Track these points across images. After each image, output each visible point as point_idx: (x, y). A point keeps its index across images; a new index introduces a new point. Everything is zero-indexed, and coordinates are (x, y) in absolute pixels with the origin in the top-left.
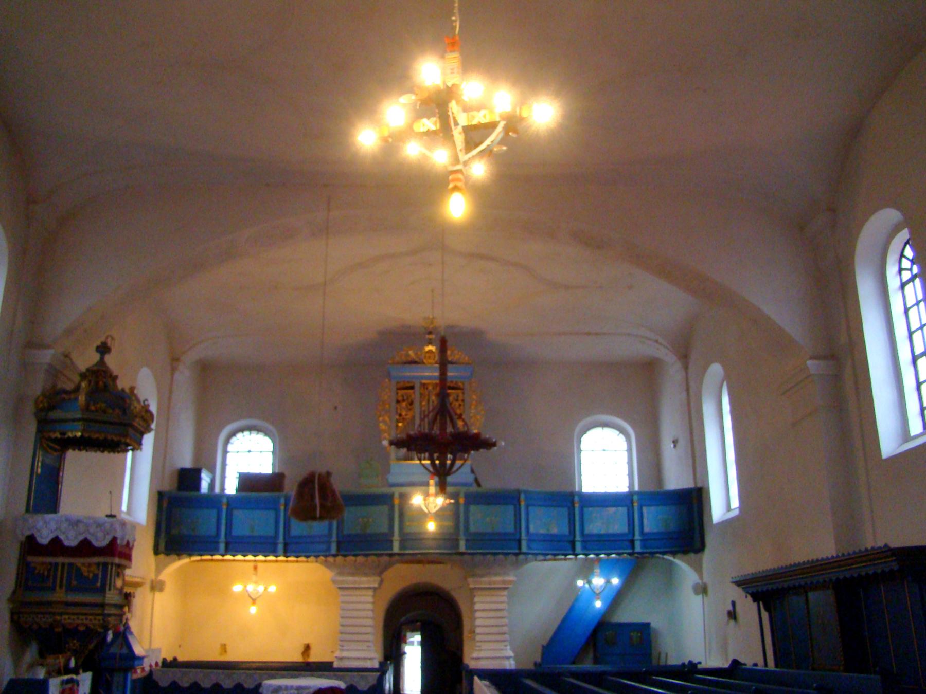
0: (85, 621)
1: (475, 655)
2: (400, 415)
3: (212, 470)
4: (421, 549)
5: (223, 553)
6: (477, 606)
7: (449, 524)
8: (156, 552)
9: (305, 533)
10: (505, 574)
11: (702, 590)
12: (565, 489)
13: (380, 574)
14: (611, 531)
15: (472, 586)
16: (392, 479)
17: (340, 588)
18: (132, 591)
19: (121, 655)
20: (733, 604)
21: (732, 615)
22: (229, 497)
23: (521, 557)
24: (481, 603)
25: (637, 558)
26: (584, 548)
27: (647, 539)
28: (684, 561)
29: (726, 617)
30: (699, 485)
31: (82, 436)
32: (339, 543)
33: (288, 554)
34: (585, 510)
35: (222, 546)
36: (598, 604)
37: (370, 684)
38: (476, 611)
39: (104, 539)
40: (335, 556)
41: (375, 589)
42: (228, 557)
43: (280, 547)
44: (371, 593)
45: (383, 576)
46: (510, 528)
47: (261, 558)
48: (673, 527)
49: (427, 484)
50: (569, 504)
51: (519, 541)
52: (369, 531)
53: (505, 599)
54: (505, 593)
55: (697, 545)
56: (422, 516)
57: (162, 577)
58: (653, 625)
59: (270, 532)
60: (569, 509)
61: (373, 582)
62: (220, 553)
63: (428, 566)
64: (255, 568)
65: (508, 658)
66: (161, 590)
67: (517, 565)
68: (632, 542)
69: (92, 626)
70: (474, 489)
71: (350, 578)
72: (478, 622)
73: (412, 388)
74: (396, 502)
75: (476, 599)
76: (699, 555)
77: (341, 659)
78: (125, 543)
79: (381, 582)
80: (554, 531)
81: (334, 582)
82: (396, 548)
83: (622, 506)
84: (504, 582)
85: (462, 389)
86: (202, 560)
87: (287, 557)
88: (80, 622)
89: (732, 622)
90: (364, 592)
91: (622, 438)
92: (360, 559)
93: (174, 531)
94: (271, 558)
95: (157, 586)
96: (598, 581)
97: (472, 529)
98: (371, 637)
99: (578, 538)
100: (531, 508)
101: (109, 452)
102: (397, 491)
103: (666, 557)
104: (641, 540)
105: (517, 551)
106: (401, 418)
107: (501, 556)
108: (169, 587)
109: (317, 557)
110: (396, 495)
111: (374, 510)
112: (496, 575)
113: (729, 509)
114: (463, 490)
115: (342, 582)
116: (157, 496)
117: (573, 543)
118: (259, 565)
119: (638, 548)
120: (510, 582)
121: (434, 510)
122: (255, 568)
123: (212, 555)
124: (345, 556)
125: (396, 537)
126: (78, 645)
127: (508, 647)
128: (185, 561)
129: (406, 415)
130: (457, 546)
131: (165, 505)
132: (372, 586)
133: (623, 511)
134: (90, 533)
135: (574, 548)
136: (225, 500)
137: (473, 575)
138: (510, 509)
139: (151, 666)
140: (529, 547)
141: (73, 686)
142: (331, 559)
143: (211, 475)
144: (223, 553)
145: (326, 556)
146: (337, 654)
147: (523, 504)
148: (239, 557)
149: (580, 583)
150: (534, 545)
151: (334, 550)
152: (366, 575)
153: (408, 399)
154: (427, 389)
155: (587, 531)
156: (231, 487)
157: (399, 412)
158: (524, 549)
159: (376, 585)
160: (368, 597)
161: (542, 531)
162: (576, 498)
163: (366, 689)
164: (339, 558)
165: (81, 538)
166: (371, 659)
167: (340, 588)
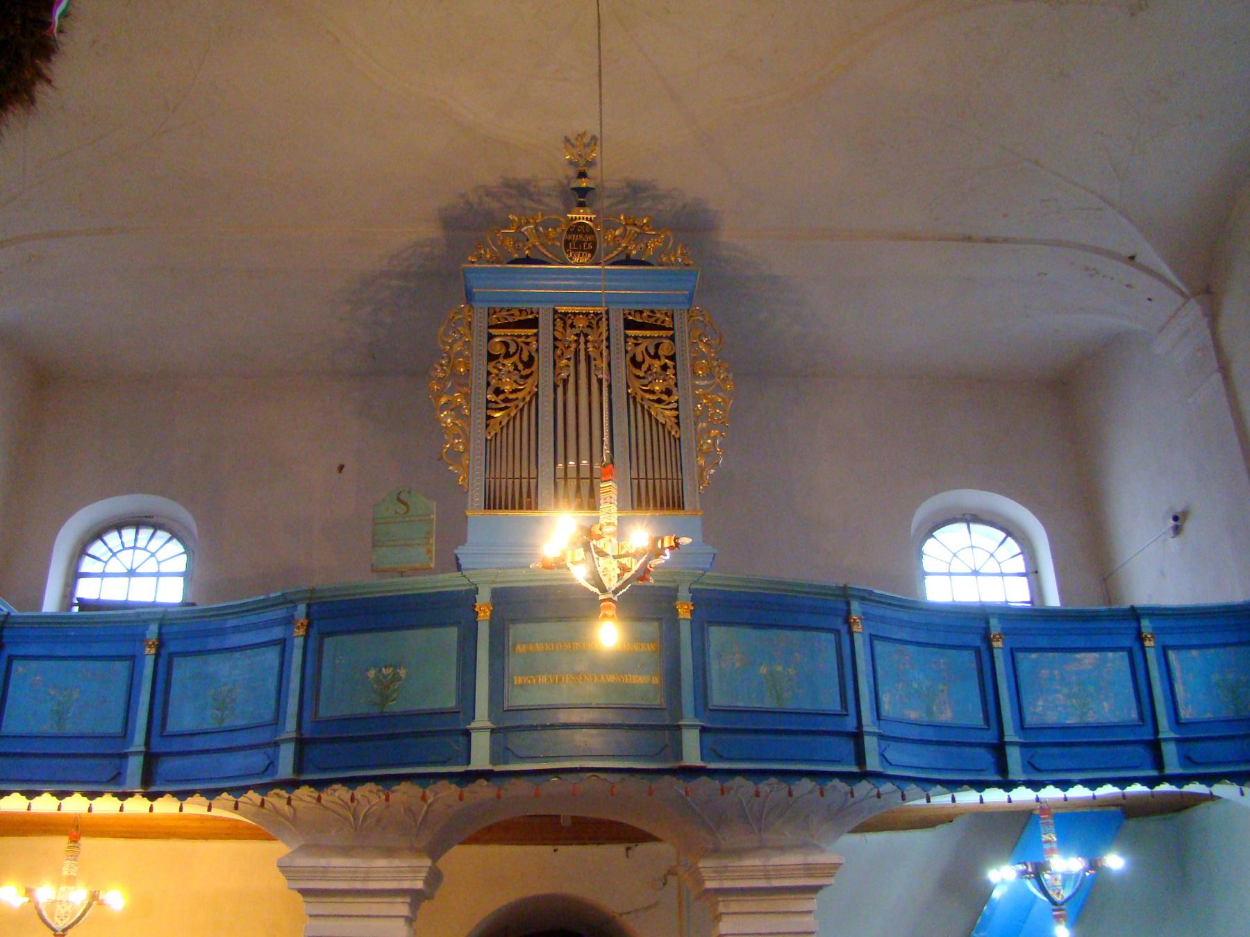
2: (498, 392)
13: (435, 852)
14: (1091, 718)
15: (709, 885)
17: (304, 892)
23: (864, 787)
26: (1030, 765)
32: (302, 744)
33: (153, 789)
34: (1020, 656)
40: (291, 785)
41: (416, 898)
43: (135, 765)
51: (857, 736)
52: (394, 707)
68: (1155, 746)
71: (338, 862)
73: (533, 323)
79: (434, 878)
81: (284, 869)
82: (481, 758)
84: (809, 869)
85: (672, 329)
91: (1012, 546)
94: (107, 805)
97: (718, 698)
105: (855, 769)
106: (502, 397)
107: (807, 784)
111: (417, 639)
112: (782, 849)
115: (314, 873)
117: (999, 749)
124: (319, 785)
129: (514, 391)
130: (679, 755)
132: (406, 885)
135: (1002, 767)
137: (716, 852)
142: (276, 799)
145: (263, 789)
152: (389, 852)
153: (519, 350)
154: (572, 326)
155: (1030, 720)
157: (493, 382)
158: (873, 763)
159: (419, 885)
161: (913, 715)
162: (995, 626)
164: (304, 792)
167: (304, 892)
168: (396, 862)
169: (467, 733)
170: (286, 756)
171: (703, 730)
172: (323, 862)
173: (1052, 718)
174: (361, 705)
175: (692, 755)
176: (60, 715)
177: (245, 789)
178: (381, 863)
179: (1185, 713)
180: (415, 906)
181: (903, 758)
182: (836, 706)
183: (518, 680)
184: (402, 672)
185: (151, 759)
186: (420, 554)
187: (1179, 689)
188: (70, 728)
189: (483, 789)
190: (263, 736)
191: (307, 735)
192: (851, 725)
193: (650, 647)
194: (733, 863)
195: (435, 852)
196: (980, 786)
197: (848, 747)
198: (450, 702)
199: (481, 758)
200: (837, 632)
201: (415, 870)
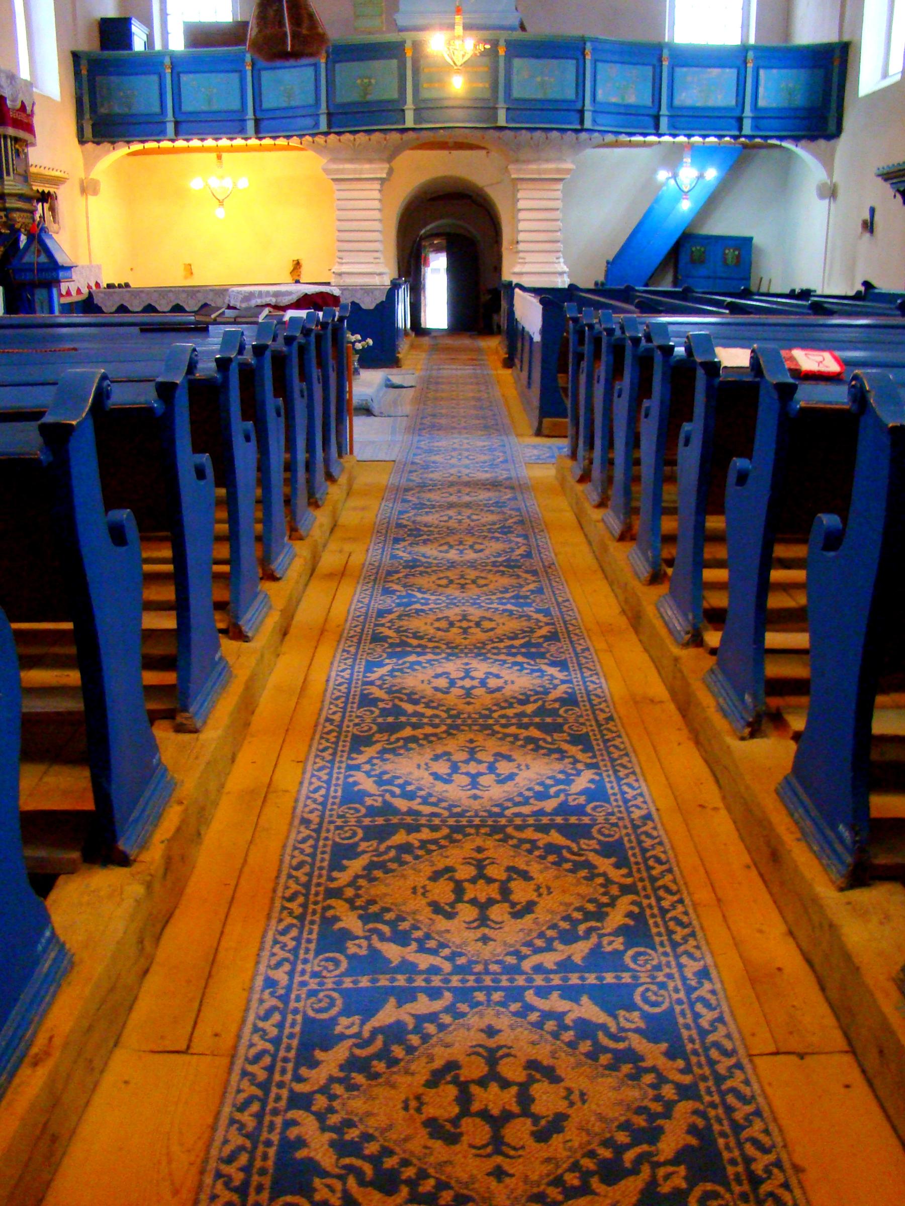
1: (517, 269)
3: (148, 23)
4: (444, 122)
5: (174, 137)
6: (521, 205)
7: (483, 85)
8: (82, 141)
9: (284, 105)
10: (560, 160)
11: (830, 193)
12: (653, 39)
13: (390, 159)
14: (711, 103)
15: (513, 176)
16: (401, 21)
18: (52, 191)
20: (872, 211)
21: (869, 226)
22: (173, 56)
23: (584, 135)
24: (526, 199)
25: (745, 146)
27: (760, 116)
28: (808, 151)
29: (860, 229)
30: (846, 38)
32: (330, 115)
35: (170, 127)
36: (686, 207)
37: (378, 301)
38: (519, 221)
40: (326, 134)
42: (180, 143)
43: (250, 125)
44: (377, 186)
45: (393, 164)
46: (570, 94)
47: (224, 142)
48: (799, 101)
49: (451, 27)
50: (655, 62)
51: (581, 112)
52: (369, 98)
53: (558, 194)
54: (560, 186)
55: (832, 128)
56: (446, 69)
57: (94, 175)
58: (758, 240)
59: (236, 105)
60: (654, 66)
61: (379, 170)
62: (169, 137)
63: (455, 153)
64: (219, 158)
65: (561, 274)
66: (95, 192)
67: (578, 146)
68: (740, 120)
70: (518, 35)
71: (348, 166)
72: (522, 226)
74: (409, 54)
75: (519, 195)
76: (833, 142)
77: (340, 274)
79: (391, 172)
80: (632, 100)
81: (325, 170)
82: (409, 123)
83: (730, 67)
84: (558, 171)
86: (144, 152)
87: (260, 139)
89: (867, 235)
90: (367, 185)
92: (361, 138)
93: (103, 110)
94: (239, 142)
95: (88, 188)
96: (688, 173)
97: (516, 94)
98: (377, 246)
99: (664, 111)
100: (600, 65)
102: (409, 37)
103: (785, 144)
104: (753, 118)
105: (579, 127)
107: (555, 134)
108: (105, 188)
109: (301, 136)
110: (408, 46)
111: (377, 65)
112: (547, 161)
113: (885, 75)
114: (503, 36)
115: (337, 171)
116: (70, 60)
117: (657, 118)
118: (225, 156)
119: (747, 130)
120: (568, 171)
121: (460, 62)
122: (219, 158)
123: (158, 141)
124: (339, 134)
125: (409, 105)
127: (562, 260)
128: (122, 151)
131: (84, 72)
132: (379, 176)
133: (730, 75)
135: (657, 126)
136: (167, 61)
137: (517, 161)
138: (571, 65)
139: (89, 287)
140: (594, 122)
142: (320, 140)
143: (146, 30)
144: (174, 137)
145: (313, 135)
146: (336, 268)
147: (588, 57)
148: (195, 143)
149: (662, 175)
150: (601, 119)
151: (323, 127)
152: (370, 161)
155: (676, 103)
156: (177, 44)
158: (588, 124)
159: (384, 176)
160: (373, 192)
161: (614, 100)
162: (666, 53)
163: (372, 307)
164: (332, 137)
166: (380, 274)
167: (334, 180)
168: (373, 166)
169: (403, 111)
170: (323, 120)
171: (508, 109)
172: (341, 166)
173: (689, 103)
174: (353, 96)
175: (502, 121)
176: (210, 101)
177: (304, 135)
178: (367, 166)
179: (761, 103)
180: (382, 185)
181: (605, 122)
182: (573, 97)
183: (425, 85)
184: (373, 81)
185: (257, 121)
186: (376, 23)
187: (761, 90)
188: (215, 108)
189: (411, 134)
190: (311, 111)
191: (332, 111)
192: (579, 106)
193: (486, 69)
194: (524, 167)
195: (390, 159)
196: (645, 135)
197: (575, 117)
198: (395, 96)
199: (409, 123)
200: (577, 59)
201: (382, 169)
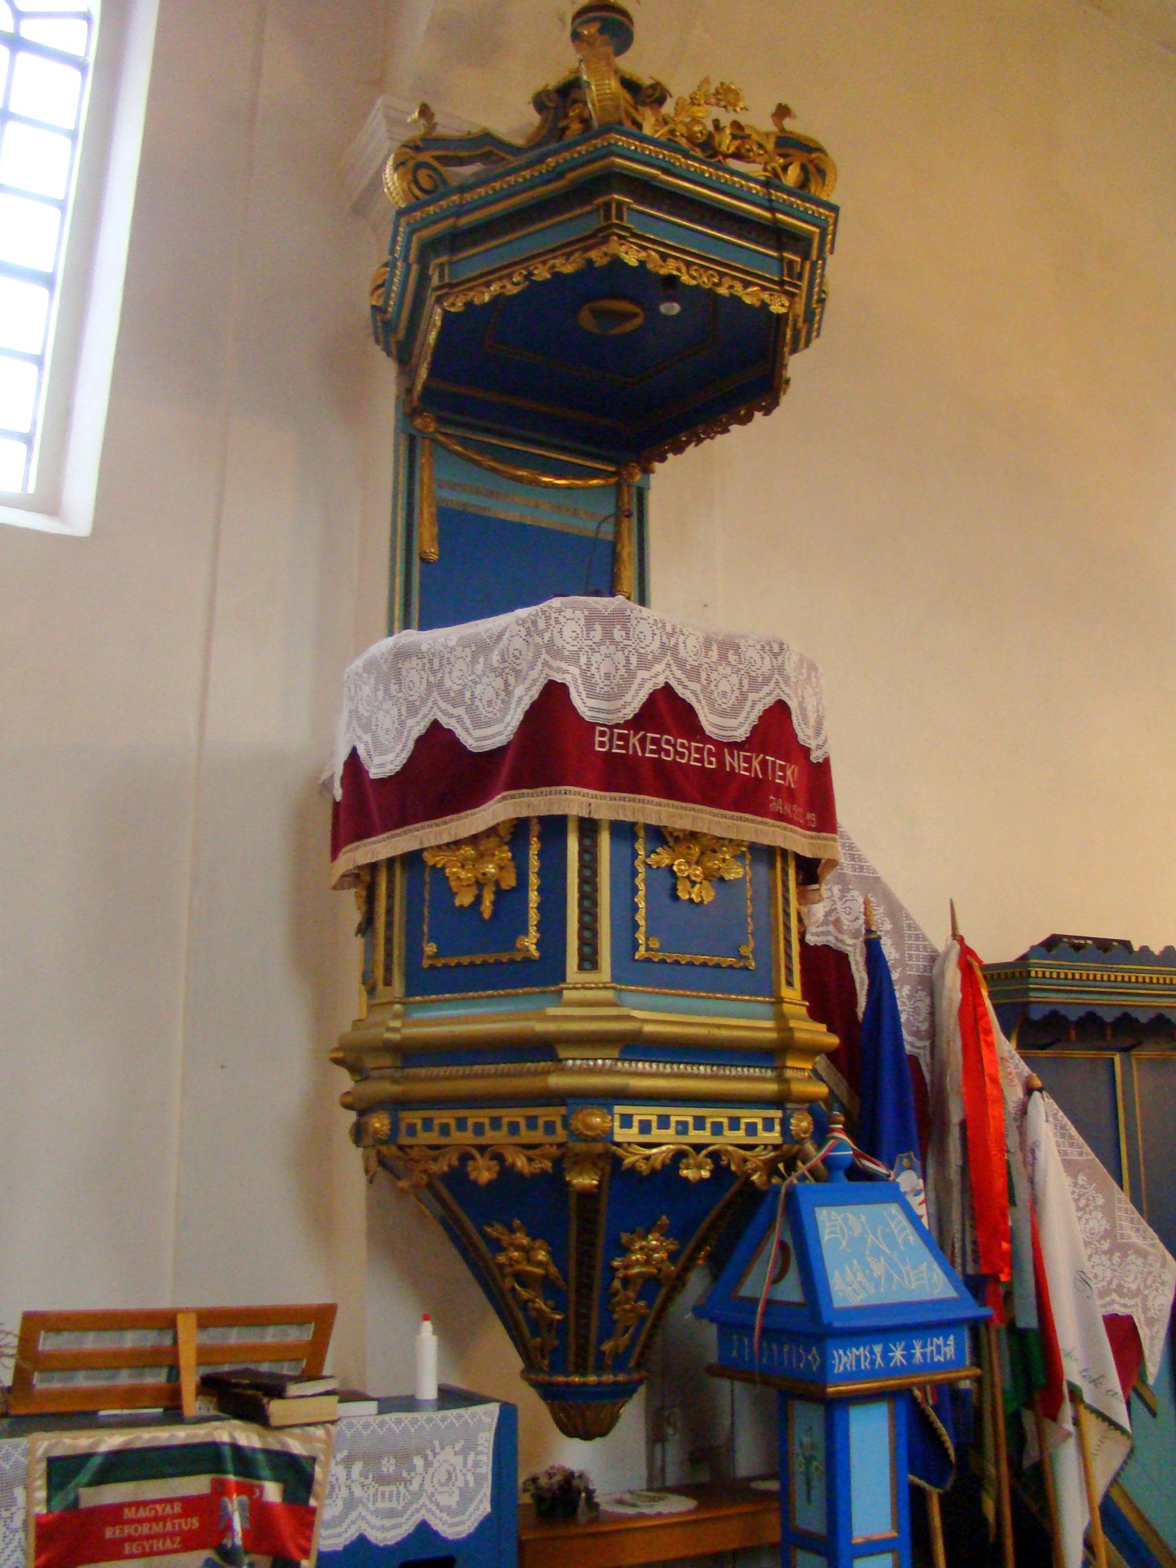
0: (490, 1136)
19: (770, 1303)
31: (446, 315)
39: (505, 711)
69: (521, 1163)
78: (632, 703)
88: (467, 1137)
101: (767, 412)
126: (542, 1256)
134: (445, 696)
141: (220, 1490)
165: (418, 727)
